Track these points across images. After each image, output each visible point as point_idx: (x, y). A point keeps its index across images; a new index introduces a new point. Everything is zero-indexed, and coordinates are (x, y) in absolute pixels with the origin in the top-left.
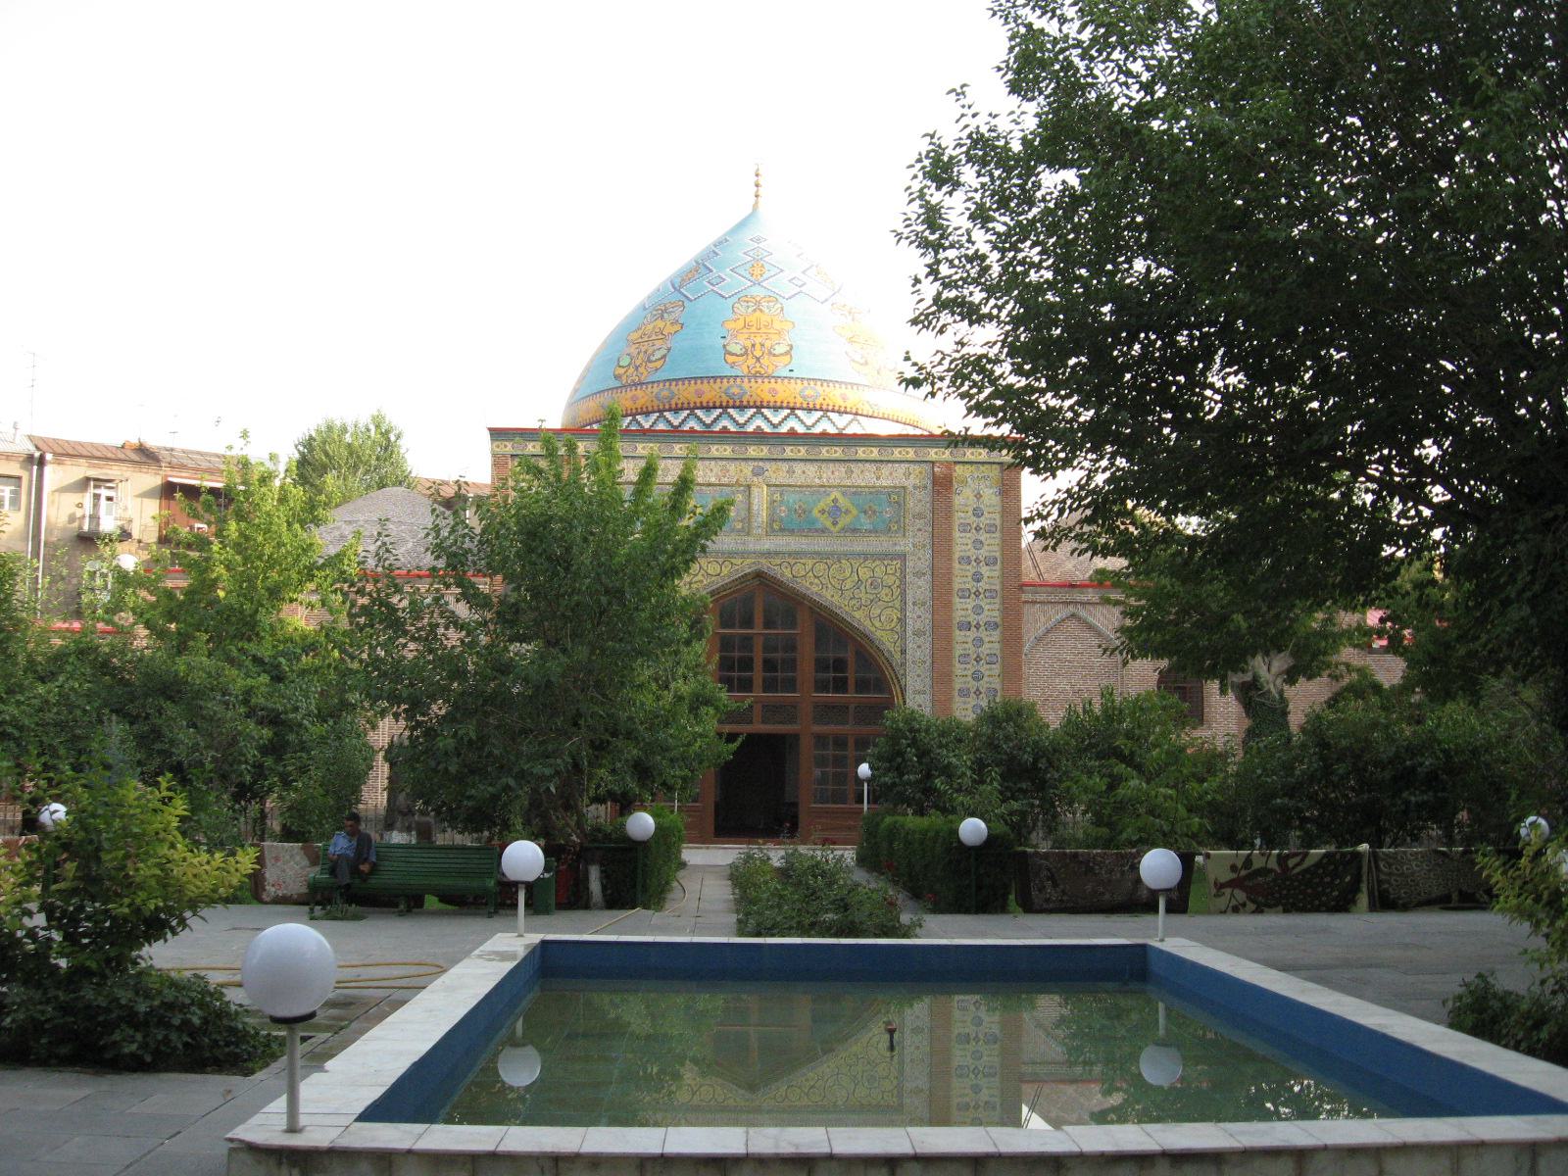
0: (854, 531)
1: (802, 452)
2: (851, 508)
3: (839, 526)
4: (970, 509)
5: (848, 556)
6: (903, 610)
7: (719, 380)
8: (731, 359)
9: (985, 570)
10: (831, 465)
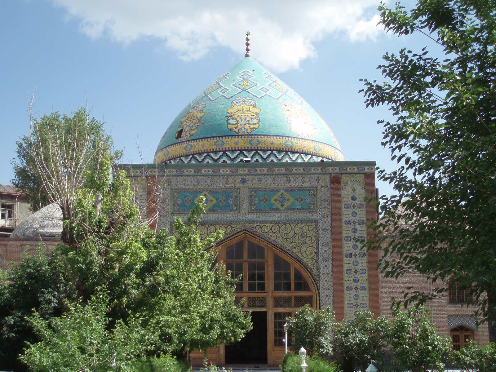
0: (292, 209)
3: (285, 207)
4: (350, 197)
5: (289, 222)
6: (317, 248)
9: (358, 227)
10: (280, 176)
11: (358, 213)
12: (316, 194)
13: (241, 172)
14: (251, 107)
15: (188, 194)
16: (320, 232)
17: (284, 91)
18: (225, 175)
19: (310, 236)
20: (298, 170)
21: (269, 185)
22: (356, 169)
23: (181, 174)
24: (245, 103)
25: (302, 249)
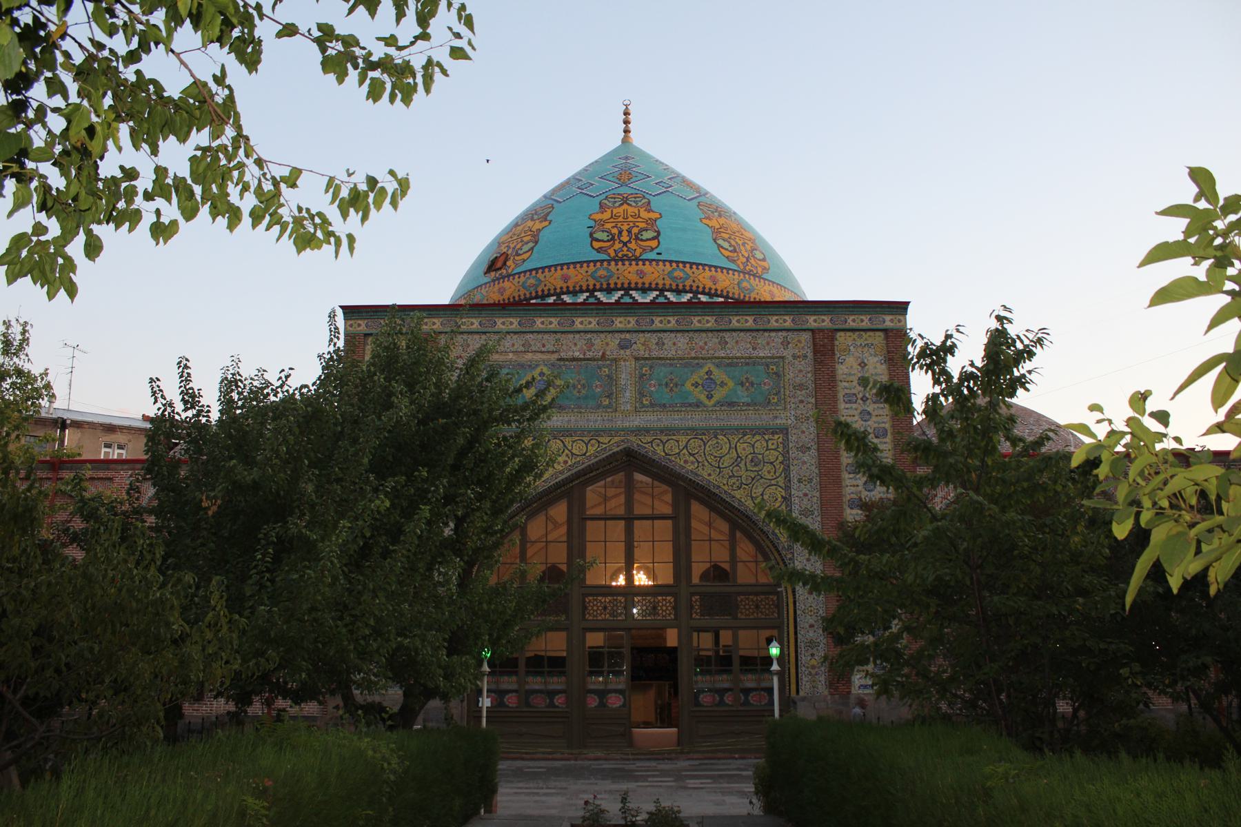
0: (731, 404)
1: (672, 322)
2: (727, 380)
4: (855, 379)
5: (724, 431)
6: (787, 488)
7: (585, 265)
8: (596, 245)
10: (704, 335)
12: (781, 373)
13: (619, 325)
14: (642, 210)
16: (793, 453)
18: (586, 332)
19: (772, 463)
20: (742, 321)
21: (679, 352)
22: (866, 321)
23: (490, 330)
24: (628, 204)
25: (754, 491)
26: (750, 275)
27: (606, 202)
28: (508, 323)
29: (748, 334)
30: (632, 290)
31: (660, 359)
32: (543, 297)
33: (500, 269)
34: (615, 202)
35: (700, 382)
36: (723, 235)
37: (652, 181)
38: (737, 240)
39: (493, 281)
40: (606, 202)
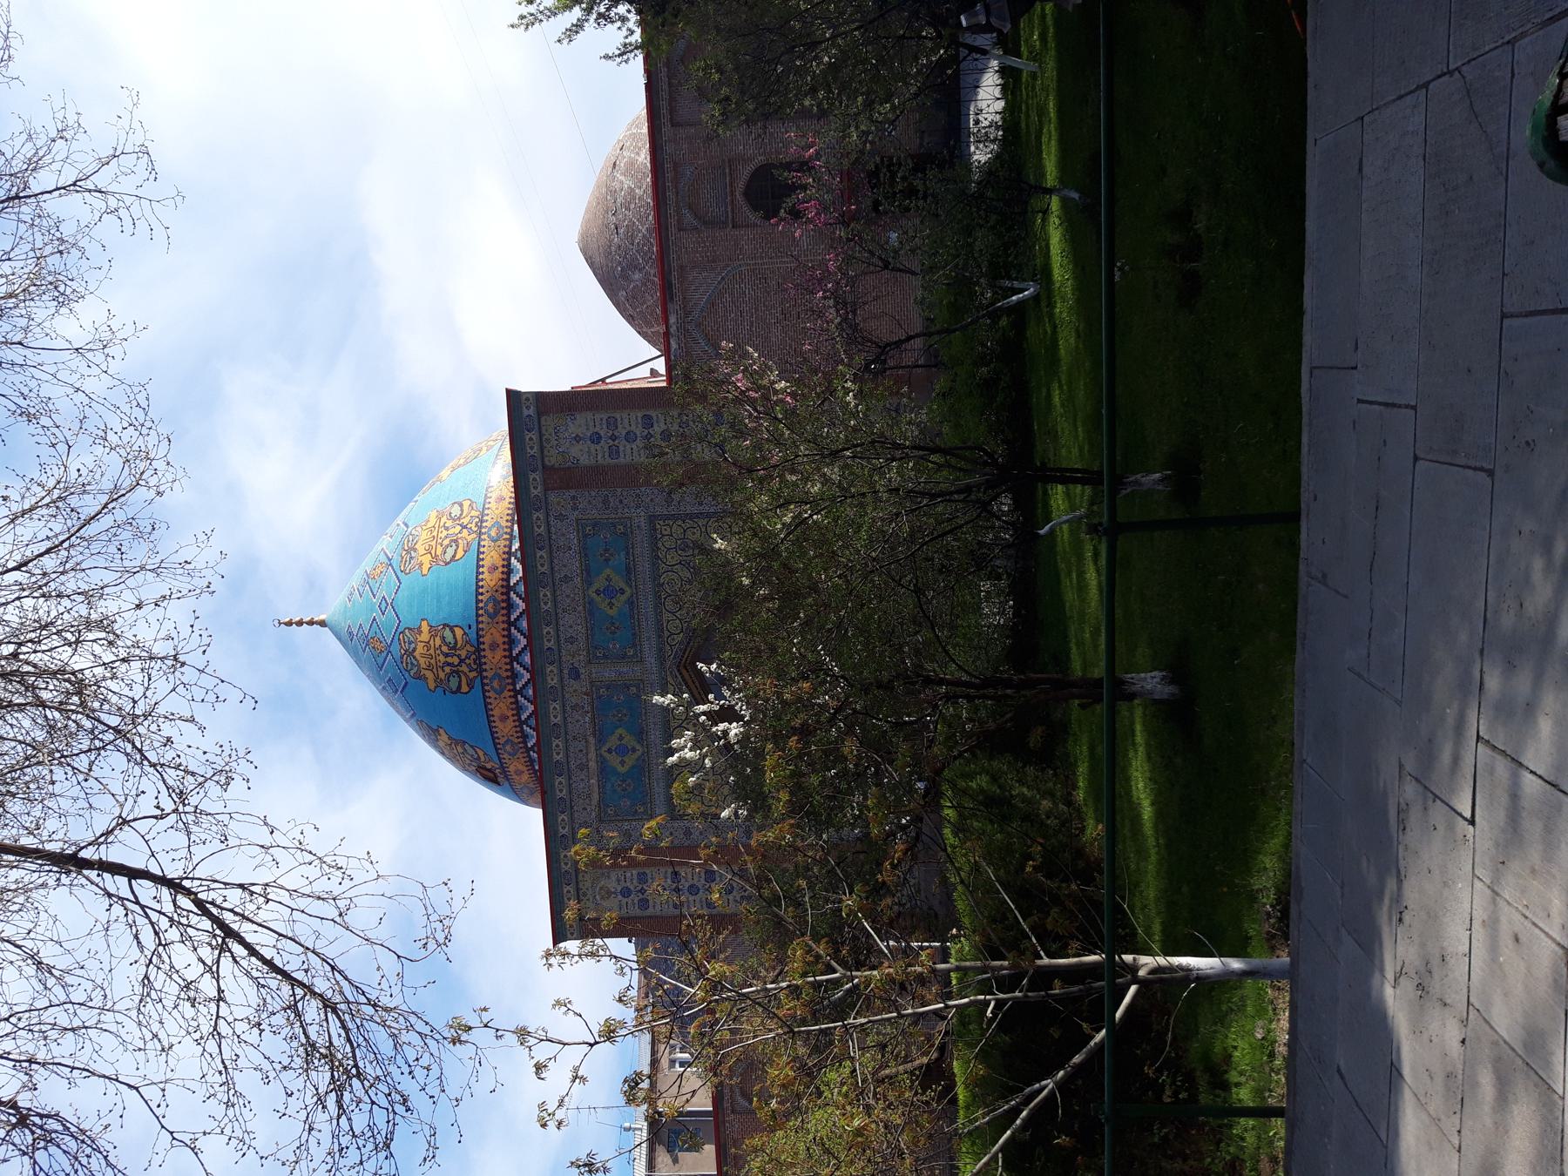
4: (593, 447)
5: (656, 577)
6: (709, 516)
7: (488, 700)
8: (465, 688)
10: (559, 598)
11: (628, 428)
15: (609, 786)
17: (387, 561)
18: (564, 712)
20: (542, 561)
24: (414, 650)
26: (481, 527)
27: (412, 673)
28: (561, 786)
29: (555, 555)
30: (511, 654)
31: (587, 639)
32: (532, 761)
33: (495, 774)
34: (412, 663)
35: (608, 601)
36: (439, 553)
37: (382, 619)
38: (443, 535)
39: (508, 780)
40: (412, 673)
